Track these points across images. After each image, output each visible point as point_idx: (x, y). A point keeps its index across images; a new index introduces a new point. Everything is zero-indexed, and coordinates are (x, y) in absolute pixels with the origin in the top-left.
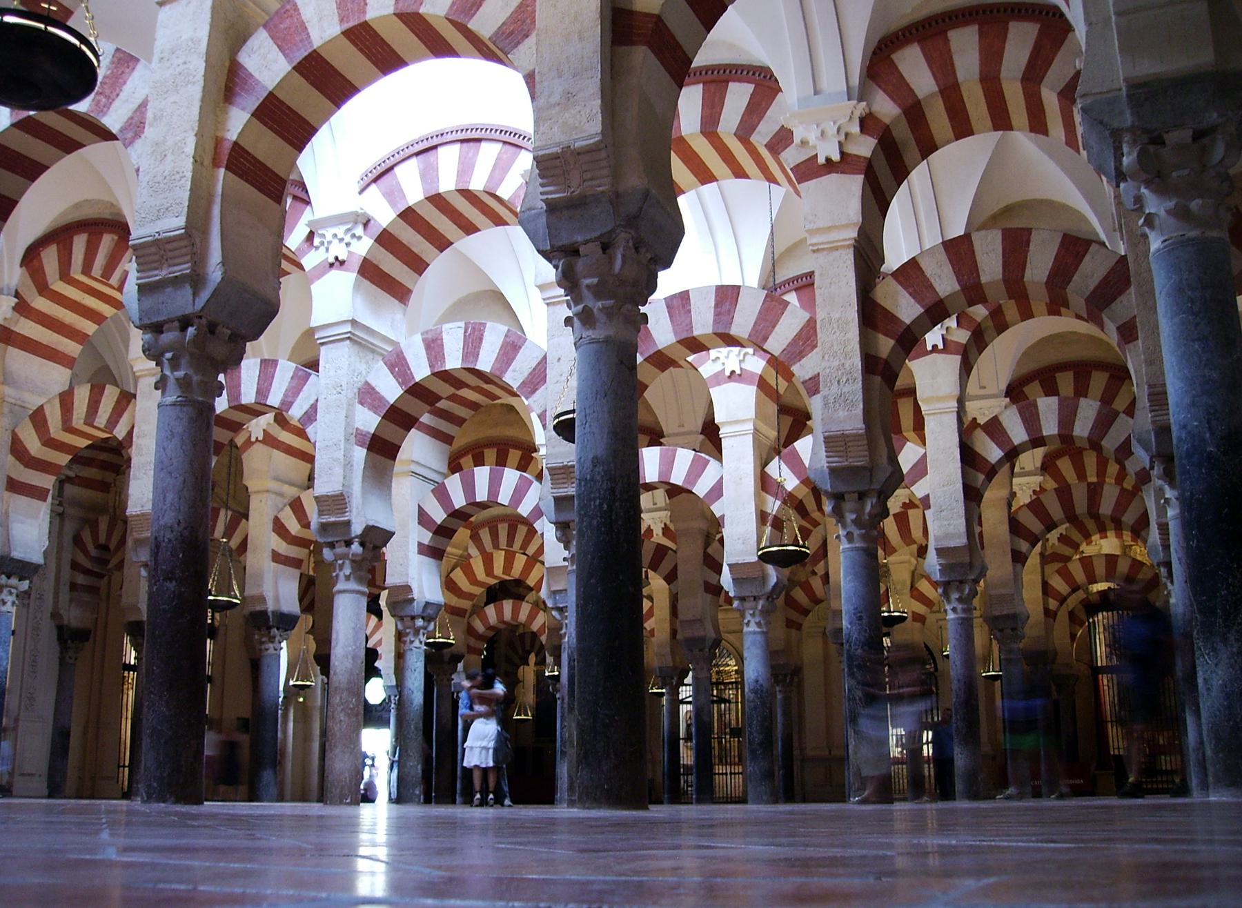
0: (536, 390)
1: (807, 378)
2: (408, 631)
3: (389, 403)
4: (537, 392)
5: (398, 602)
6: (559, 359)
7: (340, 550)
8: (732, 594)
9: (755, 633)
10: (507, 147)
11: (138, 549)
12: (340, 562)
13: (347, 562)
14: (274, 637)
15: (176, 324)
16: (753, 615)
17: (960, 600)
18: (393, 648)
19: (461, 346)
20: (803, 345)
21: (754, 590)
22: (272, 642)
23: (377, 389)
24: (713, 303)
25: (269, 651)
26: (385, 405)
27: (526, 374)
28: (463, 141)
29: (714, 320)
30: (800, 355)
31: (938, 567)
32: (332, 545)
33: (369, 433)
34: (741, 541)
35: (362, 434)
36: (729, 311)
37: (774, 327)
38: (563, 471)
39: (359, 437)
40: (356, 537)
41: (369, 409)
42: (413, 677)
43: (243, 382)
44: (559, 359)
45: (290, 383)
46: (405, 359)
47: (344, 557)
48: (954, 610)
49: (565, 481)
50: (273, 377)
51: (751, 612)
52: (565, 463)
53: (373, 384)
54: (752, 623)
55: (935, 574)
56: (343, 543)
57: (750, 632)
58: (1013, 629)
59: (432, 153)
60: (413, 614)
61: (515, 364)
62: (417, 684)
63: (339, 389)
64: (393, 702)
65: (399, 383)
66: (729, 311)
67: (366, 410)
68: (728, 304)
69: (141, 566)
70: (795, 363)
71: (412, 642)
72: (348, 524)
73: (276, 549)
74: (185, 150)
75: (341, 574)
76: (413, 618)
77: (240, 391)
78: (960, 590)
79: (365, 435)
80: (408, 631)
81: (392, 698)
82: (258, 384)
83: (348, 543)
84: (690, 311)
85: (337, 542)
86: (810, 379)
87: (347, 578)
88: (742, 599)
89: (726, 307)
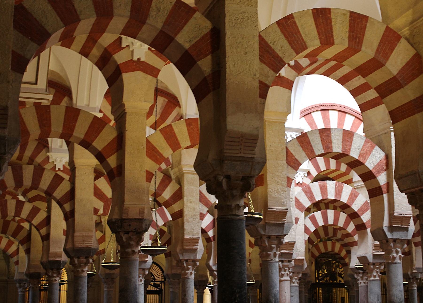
0: (364, 213)
3: (305, 207)
4: (364, 214)
9: (296, 286)
10: (357, 119)
11: (184, 254)
23: (300, 201)
26: (304, 208)
28: (339, 111)
47: (287, 266)
56: (287, 261)
58: (304, 279)
59: (327, 111)
60: (145, 268)
65: (309, 200)
69: (184, 261)
72: (292, 253)
83: (289, 261)
88: (293, 273)
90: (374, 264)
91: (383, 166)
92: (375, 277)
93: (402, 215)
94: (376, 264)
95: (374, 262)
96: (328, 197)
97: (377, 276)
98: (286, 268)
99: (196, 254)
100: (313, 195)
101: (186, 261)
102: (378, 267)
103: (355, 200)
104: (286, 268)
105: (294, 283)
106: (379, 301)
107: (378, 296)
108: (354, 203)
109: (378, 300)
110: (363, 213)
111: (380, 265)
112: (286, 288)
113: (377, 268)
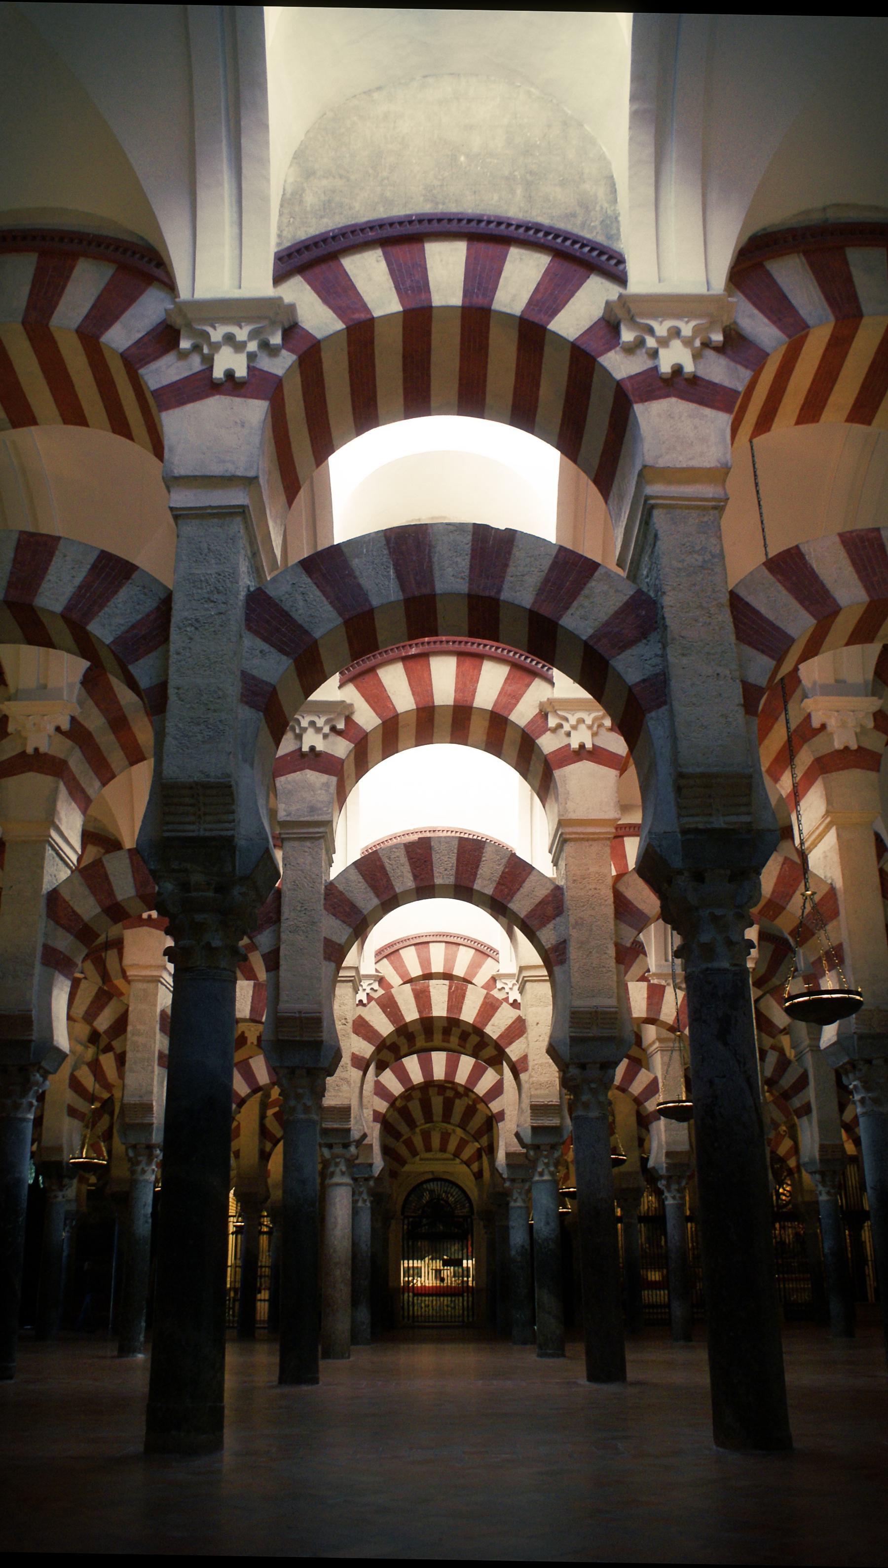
7: (338, 1150)
8: (505, 1176)
15: (598, 1065)
17: (678, 1191)
19: (446, 999)
24: (645, 995)
27: (503, 1029)
29: (648, 1008)
31: (665, 1165)
32: (330, 1146)
33: (364, 1058)
46: (396, 1003)
48: (674, 1198)
54: (519, 1200)
61: (494, 1020)
63: (344, 1021)
72: (348, 1130)
73: (72, 1104)
74: (608, 952)
82: (252, 1002)
83: (346, 1146)
87: (343, 1173)
88: (513, 1181)
90: (537, 1147)
91: (271, 915)
92: (541, 1174)
93: (297, 1015)
99: (151, 1134)
101: (134, 1147)
103: (492, 1016)
104: (338, 1160)
105: (515, 1201)
107: (548, 1214)
108: (490, 1023)
109: (548, 1223)
112: (337, 1200)
113: (546, 1157)
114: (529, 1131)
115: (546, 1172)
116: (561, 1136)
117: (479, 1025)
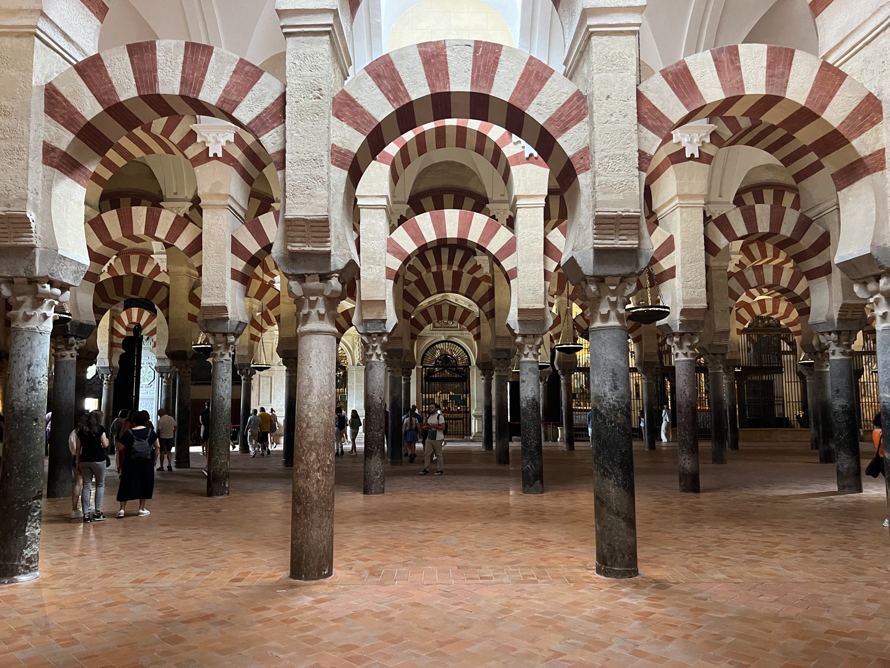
0: (567, 129)
1: (867, 154)
2: (219, 345)
5: (212, 320)
6: (608, 97)
12: (313, 298)
13: (321, 299)
14: (72, 345)
16: (531, 349)
18: (107, 339)
20: (862, 120)
21: (535, 330)
22: (70, 350)
23: (359, 102)
24: (765, 64)
25: (66, 358)
26: (371, 123)
27: (554, 110)
30: (860, 130)
31: (679, 323)
34: (531, 292)
35: (340, 153)
36: (783, 74)
37: (832, 97)
38: (612, 221)
39: (338, 156)
40: (337, 271)
41: (349, 124)
42: (224, 386)
43: (159, 66)
44: (608, 97)
45: (231, 77)
48: (686, 355)
49: (612, 232)
50: (206, 67)
51: (530, 346)
52: (620, 213)
53: (353, 94)
55: (676, 327)
57: (529, 362)
61: (540, 98)
62: (227, 392)
63: (317, 93)
64: (106, 379)
65: (389, 99)
66: (783, 74)
67: (345, 125)
68: (781, 66)
70: (855, 138)
71: (222, 355)
75: (314, 312)
76: (225, 335)
77: (155, 77)
78: (691, 340)
79: (345, 155)
80: (219, 345)
81: (105, 376)
82: (183, 72)
83: (324, 278)
84: (739, 68)
85: (309, 275)
86: (870, 155)
87: (321, 317)
88: (524, 336)
89: (779, 69)
92: (605, 318)
94: (607, 281)
95: (601, 272)
96: (449, 87)
97: (613, 314)
98: (313, 298)
100: (403, 85)
102: (613, 288)
105: (526, 356)
106: (616, 392)
108: (535, 101)
110: (564, 130)
111: (621, 281)
113: (613, 293)
114: (591, 256)
115: (613, 314)
116: (637, 265)
117: (518, 104)
